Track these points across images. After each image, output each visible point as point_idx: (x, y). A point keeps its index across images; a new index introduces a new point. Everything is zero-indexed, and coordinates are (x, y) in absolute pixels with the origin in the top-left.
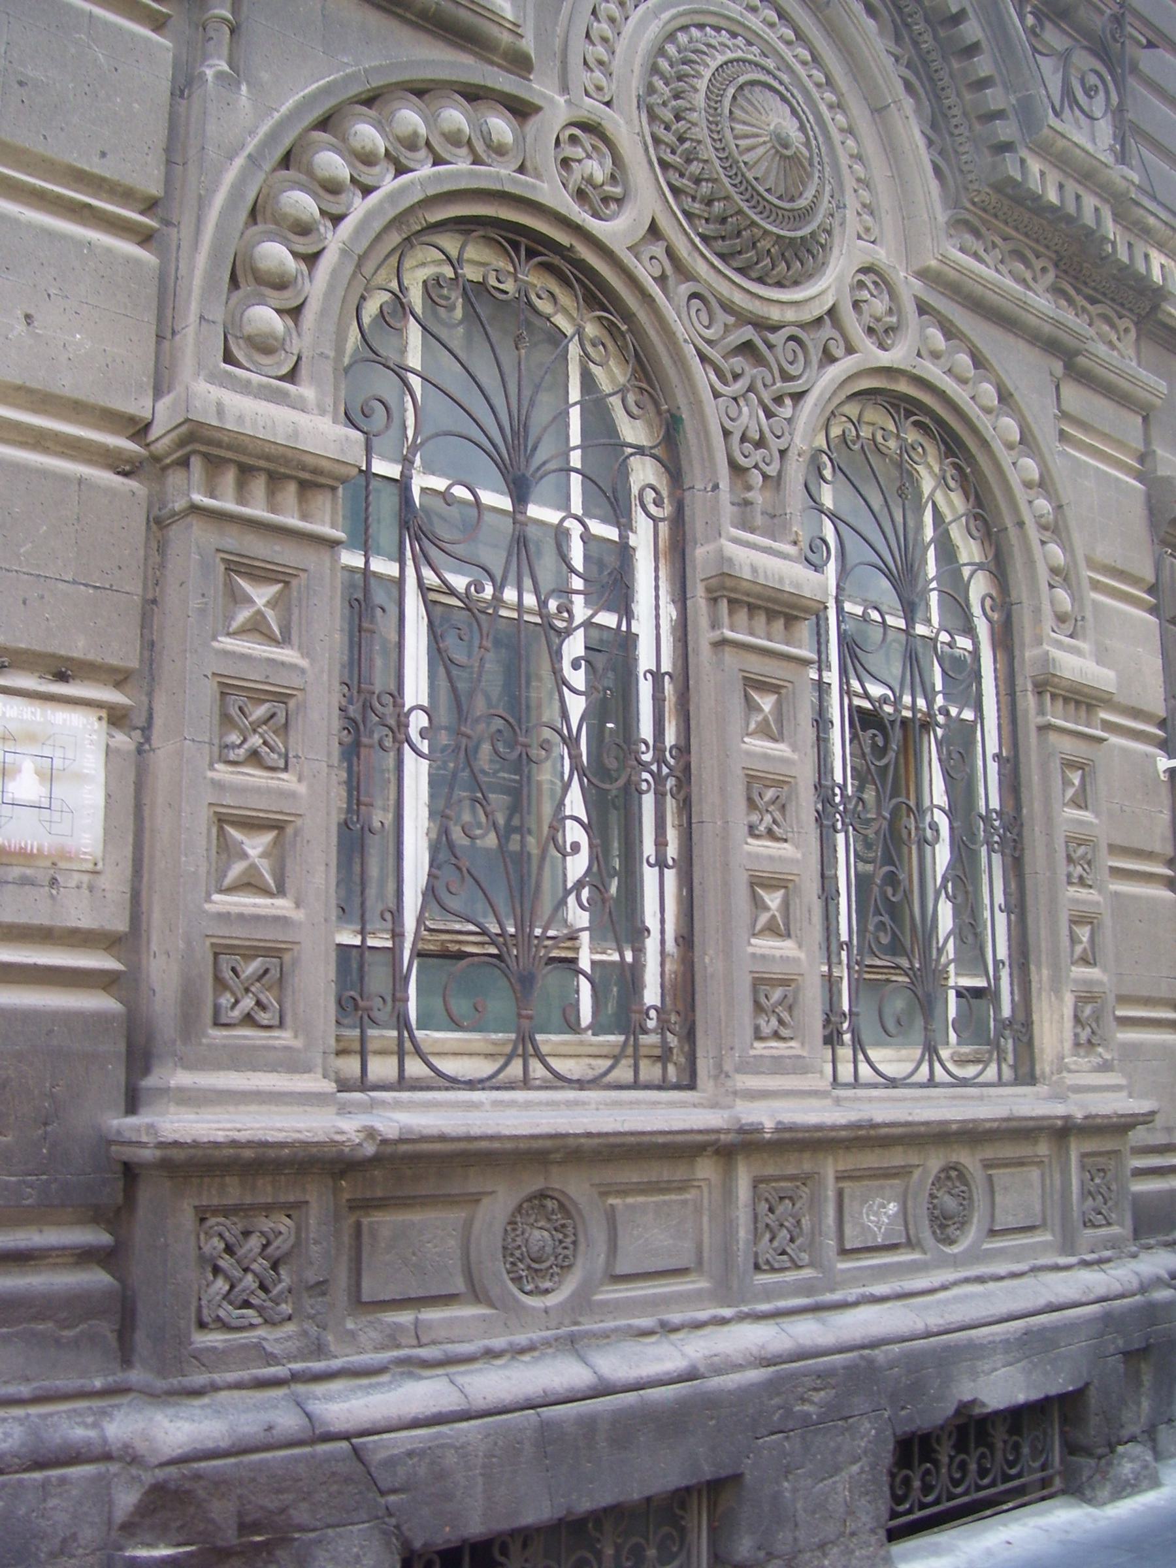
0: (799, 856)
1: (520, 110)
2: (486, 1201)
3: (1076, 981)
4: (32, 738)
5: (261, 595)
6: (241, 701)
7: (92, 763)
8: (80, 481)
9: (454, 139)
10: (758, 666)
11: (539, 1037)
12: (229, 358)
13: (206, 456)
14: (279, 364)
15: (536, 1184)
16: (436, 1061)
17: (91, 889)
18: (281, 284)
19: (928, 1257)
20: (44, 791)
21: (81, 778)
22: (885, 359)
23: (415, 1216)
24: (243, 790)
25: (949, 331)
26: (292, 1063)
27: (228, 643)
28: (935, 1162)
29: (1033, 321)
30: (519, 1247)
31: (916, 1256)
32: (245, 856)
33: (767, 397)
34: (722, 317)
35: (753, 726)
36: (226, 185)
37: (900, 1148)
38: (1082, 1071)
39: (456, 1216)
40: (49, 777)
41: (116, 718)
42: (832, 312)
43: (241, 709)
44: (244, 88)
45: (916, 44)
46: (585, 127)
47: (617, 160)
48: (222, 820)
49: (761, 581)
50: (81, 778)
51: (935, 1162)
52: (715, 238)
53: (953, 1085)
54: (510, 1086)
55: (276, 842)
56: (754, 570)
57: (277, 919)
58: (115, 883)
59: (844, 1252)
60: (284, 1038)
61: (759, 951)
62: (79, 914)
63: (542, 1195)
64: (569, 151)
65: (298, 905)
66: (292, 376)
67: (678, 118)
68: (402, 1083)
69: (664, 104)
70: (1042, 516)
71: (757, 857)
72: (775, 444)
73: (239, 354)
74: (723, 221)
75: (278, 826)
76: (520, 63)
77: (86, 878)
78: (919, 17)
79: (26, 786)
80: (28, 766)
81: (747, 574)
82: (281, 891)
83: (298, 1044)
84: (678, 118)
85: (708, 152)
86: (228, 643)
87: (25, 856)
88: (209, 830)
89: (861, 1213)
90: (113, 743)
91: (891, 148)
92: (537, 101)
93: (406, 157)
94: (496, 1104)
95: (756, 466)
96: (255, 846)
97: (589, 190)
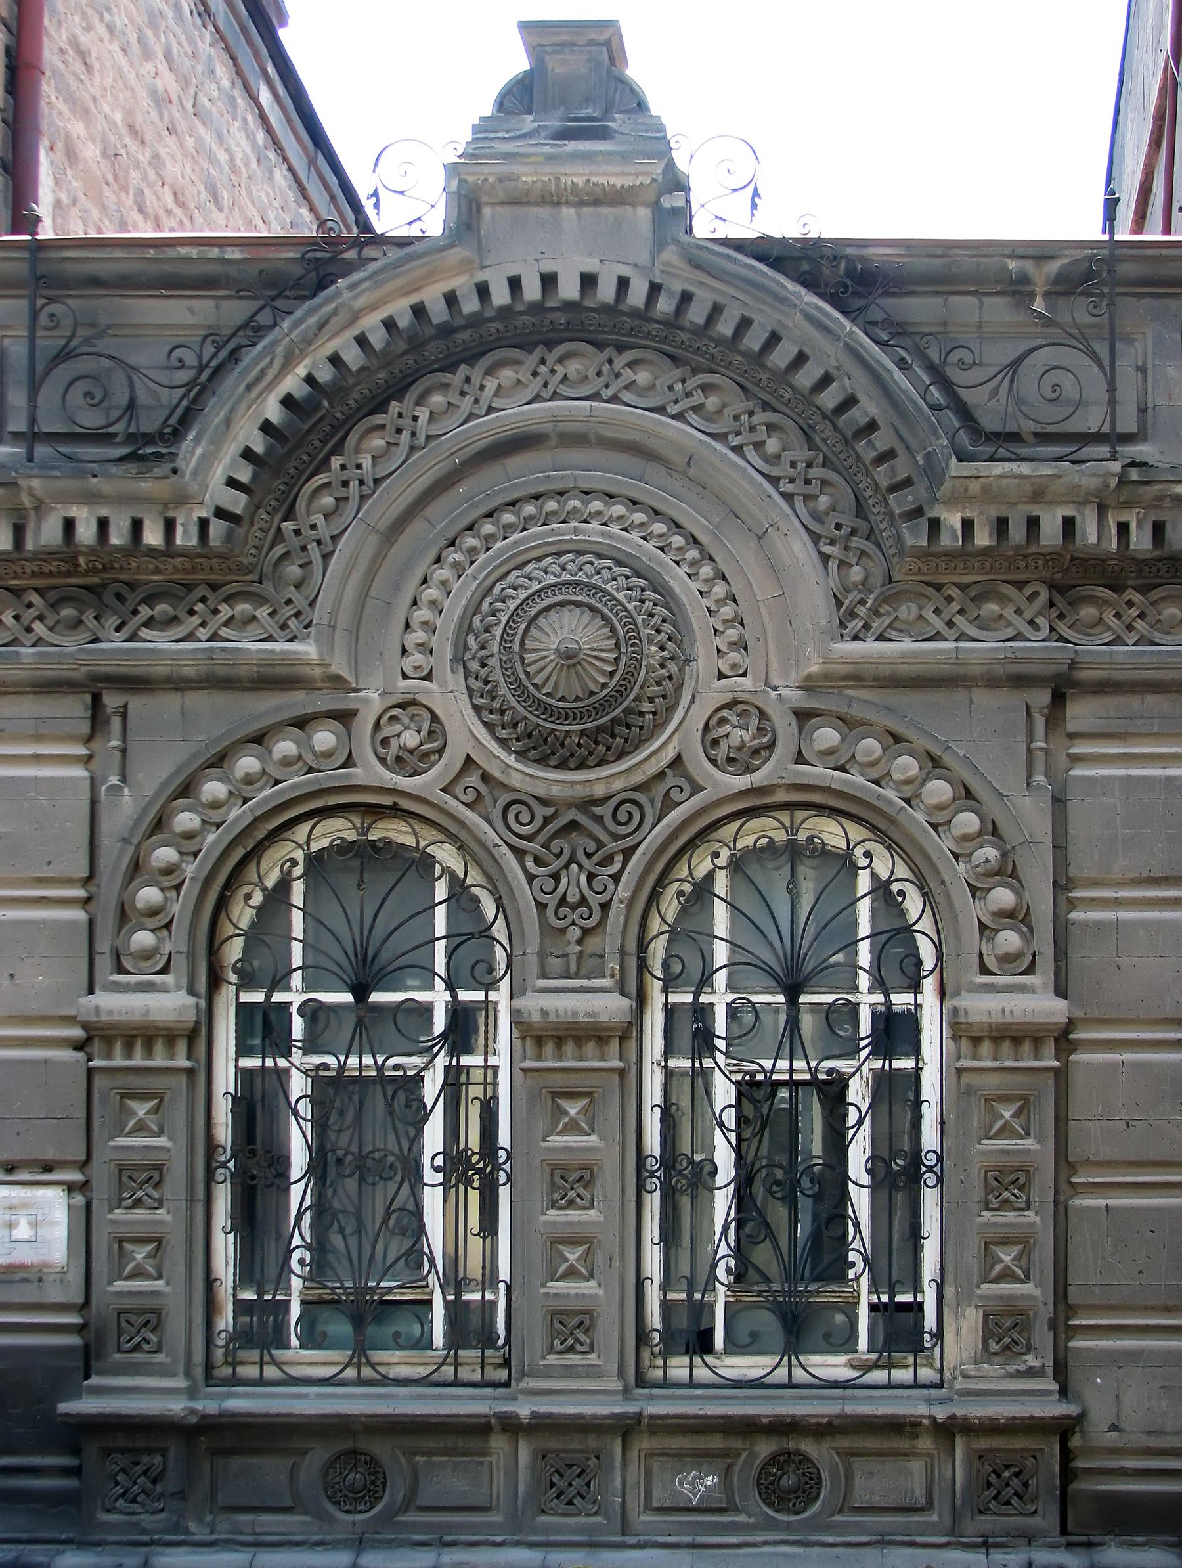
0: (602, 1218)
1: (345, 717)
2: (309, 1454)
3: (981, 1297)
4: (25, 1205)
5: (141, 1109)
6: (129, 1173)
7: (60, 1215)
8: (46, 1061)
9: (287, 762)
10: (559, 1081)
11: (369, 1352)
12: (121, 970)
13: (101, 1036)
14: (156, 964)
15: (349, 1444)
16: (285, 1368)
17: (62, 1281)
18: (154, 912)
19: (752, 1520)
20: (33, 1233)
21: (55, 1224)
22: (742, 782)
23: (257, 1460)
24: (140, 1222)
25: (846, 723)
26: (163, 1371)
27: (122, 1141)
28: (765, 1448)
29: (977, 670)
30: (338, 1483)
31: (742, 1518)
32: (134, 1259)
33: (586, 863)
34: (541, 811)
35: (561, 1126)
36: (114, 858)
37: (721, 1435)
38: (993, 1375)
39: (286, 1462)
40: (35, 1225)
41: (70, 1188)
42: (678, 760)
43: (130, 1177)
44: (126, 791)
45: (824, 440)
46: (402, 706)
47: (434, 717)
48: (121, 1241)
49: (552, 1018)
50: (55, 1224)
51: (765, 1448)
52: (529, 750)
53: (822, 1387)
54: (344, 1383)
55: (158, 1248)
56: (544, 1012)
57: (152, 1292)
58: (76, 1278)
59: (648, 1507)
60: (161, 1358)
61: (552, 1291)
62: (55, 1295)
63: (354, 1453)
64: (387, 731)
65: (168, 1284)
66: (164, 971)
67: (483, 665)
68: (261, 1382)
69: (473, 658)
70: (978, 866)
71: (554, 1223)
72: (594, 900)
73: (127, 964)
74: (529, 735)
75: (159, 1241)
76: (337, 682)
77: (58, 1276)
78: (817, 418)
79: (23, 1231)
80: (23, 1221)
81: (536, 1017)
82: (160, 1277)
83: (168, 1360)
84: (483, 665)
85: (503, 690)
86: (122, 1141)
87: (23, 1267)
88: (110, 1249)
89: (673, 1482)
90: (72, 1202)
91: (775, 569)
92: (352, 706)
93: (247, 791)
94: (319, 1395)
95: (573, 923)
96: (140, 1254)
97: (406, 756)
